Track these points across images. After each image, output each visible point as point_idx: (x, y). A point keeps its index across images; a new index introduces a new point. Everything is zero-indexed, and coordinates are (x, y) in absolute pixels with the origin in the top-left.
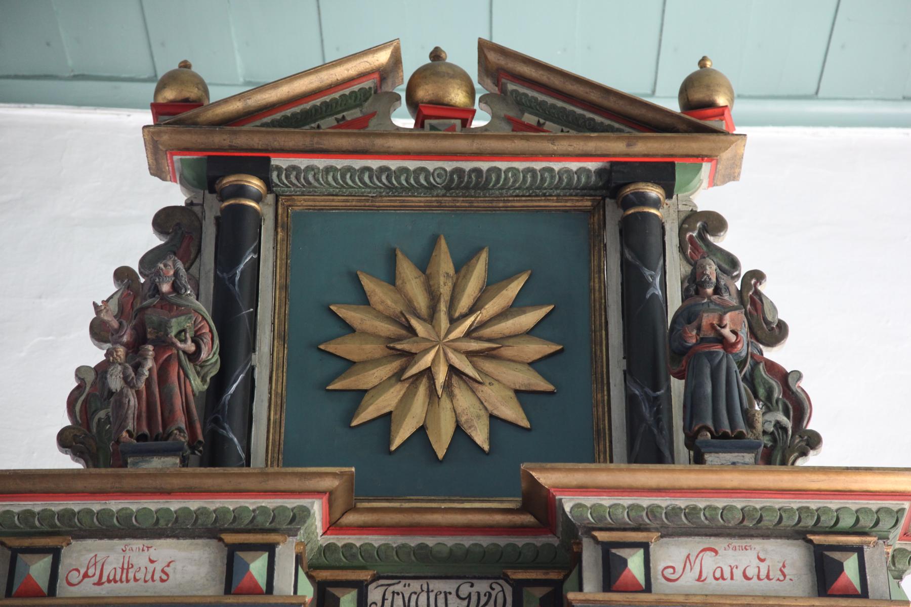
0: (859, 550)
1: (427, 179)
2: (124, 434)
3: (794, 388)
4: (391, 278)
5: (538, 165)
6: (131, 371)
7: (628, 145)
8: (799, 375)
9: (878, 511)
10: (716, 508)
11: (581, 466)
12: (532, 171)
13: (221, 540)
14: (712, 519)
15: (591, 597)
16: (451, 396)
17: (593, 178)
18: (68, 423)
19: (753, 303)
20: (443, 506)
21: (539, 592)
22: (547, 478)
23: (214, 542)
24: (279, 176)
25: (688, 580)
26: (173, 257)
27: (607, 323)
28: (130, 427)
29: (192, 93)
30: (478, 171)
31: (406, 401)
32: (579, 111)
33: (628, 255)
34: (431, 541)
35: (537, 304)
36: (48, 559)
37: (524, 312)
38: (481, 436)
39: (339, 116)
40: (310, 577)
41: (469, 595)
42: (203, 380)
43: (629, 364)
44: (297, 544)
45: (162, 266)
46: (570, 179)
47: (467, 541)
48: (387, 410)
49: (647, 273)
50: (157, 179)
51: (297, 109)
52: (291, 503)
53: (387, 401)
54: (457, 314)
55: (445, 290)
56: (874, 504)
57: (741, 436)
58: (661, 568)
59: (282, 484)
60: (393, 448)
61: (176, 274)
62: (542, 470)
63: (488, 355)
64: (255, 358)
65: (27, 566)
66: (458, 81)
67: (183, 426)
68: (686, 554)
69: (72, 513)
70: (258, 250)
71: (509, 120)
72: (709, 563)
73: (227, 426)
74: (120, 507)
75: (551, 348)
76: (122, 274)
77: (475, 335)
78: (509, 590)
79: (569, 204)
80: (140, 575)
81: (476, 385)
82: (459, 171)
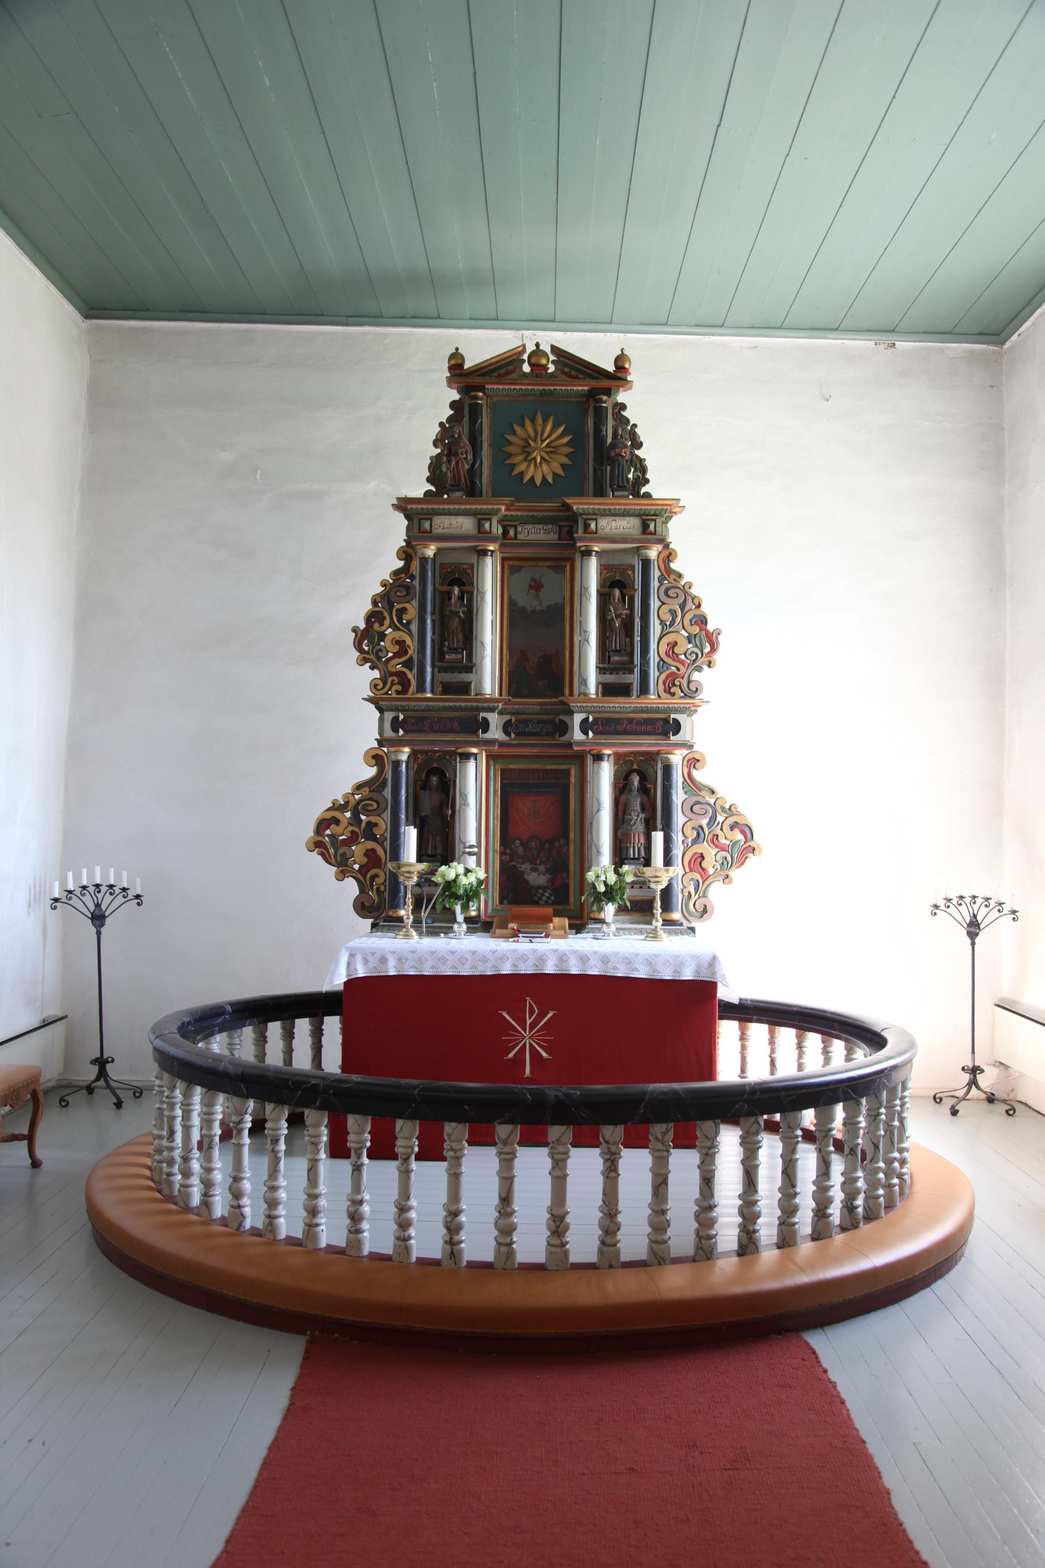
0: (655, 520)
4: (523, 426)
5: (569, 388)
8: (645, 460)
12: (567, 390)
21: (566, 529)
25: (608, 529)
29: (460, 361)
30: (550, 390)
31: (528, 467)
34: (535, 514)
35: (568, 435)
36: (429, 522)
38: (550, 479)
47: (546, 514)
49: (602, 427)
52: (496, 507)
53: (522, 467)
55: (540, 430)
56: (660, 508)
57: (625, 486)
70: (482, 418)
72: (614, 524)
76: (441, 424)
78: (557, 527)
82: (544, 390)
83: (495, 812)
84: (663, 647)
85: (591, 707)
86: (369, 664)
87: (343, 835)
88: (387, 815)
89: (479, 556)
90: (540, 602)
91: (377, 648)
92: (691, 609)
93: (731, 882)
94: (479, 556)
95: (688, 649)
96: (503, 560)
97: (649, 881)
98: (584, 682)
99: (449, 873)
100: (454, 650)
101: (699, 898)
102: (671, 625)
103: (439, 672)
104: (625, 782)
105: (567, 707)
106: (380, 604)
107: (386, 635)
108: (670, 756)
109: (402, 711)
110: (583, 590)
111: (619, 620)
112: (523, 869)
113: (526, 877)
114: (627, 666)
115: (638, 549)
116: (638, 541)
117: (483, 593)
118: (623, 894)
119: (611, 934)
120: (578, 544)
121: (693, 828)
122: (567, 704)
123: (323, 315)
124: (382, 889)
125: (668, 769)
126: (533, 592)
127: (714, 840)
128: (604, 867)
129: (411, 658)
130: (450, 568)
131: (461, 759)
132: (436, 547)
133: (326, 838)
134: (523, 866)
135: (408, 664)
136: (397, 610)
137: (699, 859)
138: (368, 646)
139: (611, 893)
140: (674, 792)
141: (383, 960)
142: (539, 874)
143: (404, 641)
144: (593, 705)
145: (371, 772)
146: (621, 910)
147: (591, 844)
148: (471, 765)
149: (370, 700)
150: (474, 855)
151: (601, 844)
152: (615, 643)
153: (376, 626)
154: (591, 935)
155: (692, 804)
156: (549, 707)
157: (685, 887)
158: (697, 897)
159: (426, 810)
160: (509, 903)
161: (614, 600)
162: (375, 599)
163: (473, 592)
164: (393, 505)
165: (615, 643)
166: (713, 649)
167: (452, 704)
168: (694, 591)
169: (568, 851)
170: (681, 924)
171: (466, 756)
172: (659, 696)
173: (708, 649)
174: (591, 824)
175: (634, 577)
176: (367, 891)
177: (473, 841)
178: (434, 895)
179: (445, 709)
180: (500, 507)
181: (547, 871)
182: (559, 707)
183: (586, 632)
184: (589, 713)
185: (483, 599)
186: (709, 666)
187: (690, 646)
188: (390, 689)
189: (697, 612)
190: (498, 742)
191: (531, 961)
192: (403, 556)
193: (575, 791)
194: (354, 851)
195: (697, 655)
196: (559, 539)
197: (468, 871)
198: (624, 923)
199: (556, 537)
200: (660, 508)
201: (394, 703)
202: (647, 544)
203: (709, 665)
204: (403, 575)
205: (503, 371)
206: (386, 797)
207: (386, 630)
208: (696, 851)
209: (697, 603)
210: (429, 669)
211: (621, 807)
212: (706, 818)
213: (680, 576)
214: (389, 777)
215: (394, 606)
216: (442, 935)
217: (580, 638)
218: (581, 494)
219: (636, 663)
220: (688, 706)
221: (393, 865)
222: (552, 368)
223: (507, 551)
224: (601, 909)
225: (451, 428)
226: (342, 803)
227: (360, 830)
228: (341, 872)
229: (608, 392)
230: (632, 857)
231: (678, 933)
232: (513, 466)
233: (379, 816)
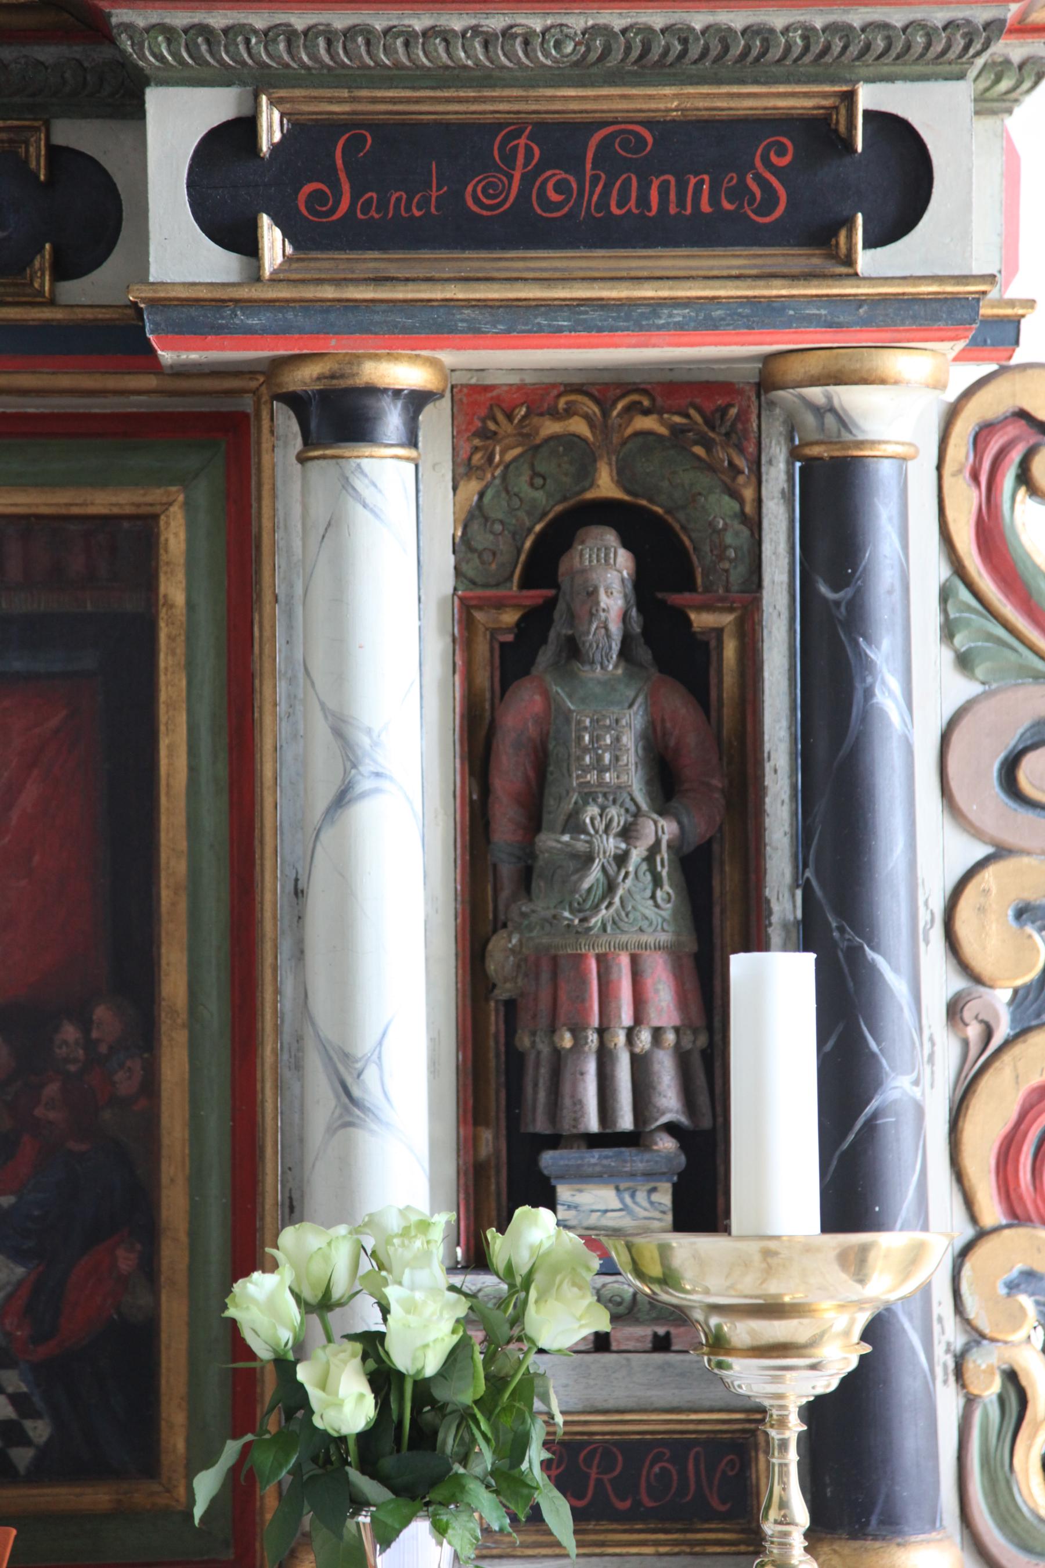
85: (268, 35)
97: (718, 1344)
104: (536, 596)
147: (299, 1039)
151: (365, 1045)
155: (1010, 741)
157: (977, 1336)
174: (299, 893)
182: (47, 53)
193: (190, 666)
230: (593, 1124)
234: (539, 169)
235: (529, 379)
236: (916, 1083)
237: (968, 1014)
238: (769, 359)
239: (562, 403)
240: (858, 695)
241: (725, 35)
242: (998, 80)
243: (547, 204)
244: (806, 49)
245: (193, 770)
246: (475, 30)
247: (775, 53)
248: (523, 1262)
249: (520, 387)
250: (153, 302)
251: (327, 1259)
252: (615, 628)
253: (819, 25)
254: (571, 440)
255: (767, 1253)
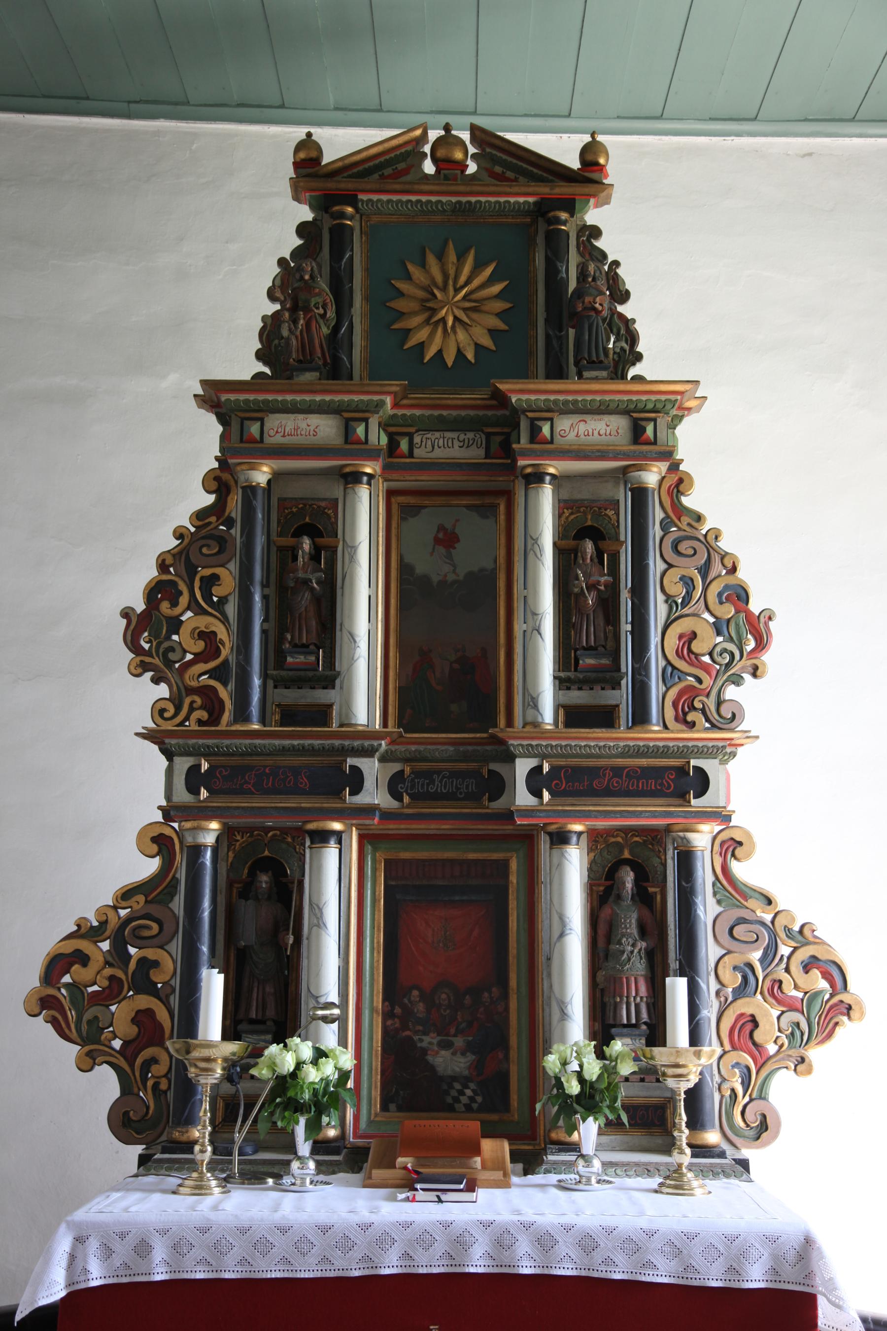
0: (655, 420)
1: (442, 206)
2: (291, 360)
3: (631, 328)
4: (423, 264)
5: (502, 199)
6: (292, 326)
7: (551, 189)
8: (634, 321)
9: (666, 400)
10: (587, 401)
11: (521, 381)
12: (499, 202)
13: (341, 415)
14: (585, 406)
15: (523, 446)
16: (455, 333)
17: (532, 207)
18: (259, 346)
19: (613, 279)
20: (451, 396)
21: (499, 439)
22: (503, 387)
23: (338, 416)
24: (362, 205)
25: (572, 436)
26: (310, 260)
27: (537, 290)
28: (294, 357)
29: (314, 154)
30: (469, 202)
31: (432, 335)
32: (525, 166)
33: (549, 254)
34: (445, 413)
35: (500, 280)
36: (258, 424)
37: (493, 285)
38: (470, 356)
39: (394, 167)
40: (385, 430)
41: (464, 440)
42: (328, 328)
43: (548, 314)
44: (379, 418)
45: (304, 265)
46: (519, 207)
47: (463, 413)
48: (422, 340)
49: (559, 264)
50: (296, 203)
51: (371, 164)
52: (376, 398)
53: (422, 335)
54: (458, 286)
55: (452, 272)
56: (663, 398)
57: (601, 362)
58: (558, 430)
59: (372, 389)
60: (425, 361)
61: (312, 269)
62: (501, 383)
63: (475, 309)
64: (353, 310)
65: (249, 428)
66: (459, 147)
67: (320, 355)
68: (570, 425)
69: (268, 401)
70: (352, 250)
71: (487, 170)
72: (582, 427)
73: (340, 351)
74: (291, 398)
75: (508, 305)
76: (282, 262)
77: (468, 298)
78: (483, 437)
79: (518, 220)
80: (303, 433)
81: (468, 327)
82: (459, 202)
83: (375, 938)
84: (672, 642)
85: (546, 746)
86: (151, 673)
87: (94, 983)
88: (176, 946)
89: (347, 483)
90: (455, 566)
91: (166, 645)
92: (719, 576)
93: (809, 1071)
94: (347, 483)
95: (716, 645)
96: (390, 494)
97: (664, 1074)
98: (533, 703)
99: (283, 1061)
100: (302, 648)
101: (751, 1100)
102: (685, 604)
103: (275, 687)
104: (609, 883)
105: (504, 747)
106: (172, 569)
107: (182, 622)
108: (690, 835)
109: (206, 755)
110: (530, 542)
111: (594, 594)
112: (424, 1044)
113: (430, 1058)
114: (608, 675)
115: (625, 470)
116: (626, 456)
117: (353, 547)
118: (615, 1100)
119: (593, 1180)
120: (521, 463)
121: (735, 968)
122: (502, 742)
123: (88, 98)
124: (164, 1086)
125: (686, 859)
126: (441, 550)
127: (775, 990)
128: (576, 1044)
129: (226, 662)
130: (297, 507)
131: (312, 842)
132: (272, 468)
133: (63, 991)
134: (424, 1037)
135: (220, 674)
136: (202, 578)
137: (749, 1027)
138: (149, 642)
139: (592, 1097)
140: (699, 900)
141: (143, 1249)
142: (454, 1054)
143: (214, 633)
144: (549, 742)
145: (151, 866)
146: (611, 1126)
147: (550, 998)
148: (331, 855)
149: (149, 736)
150: (333, 1021)
151: (568, 999)
152: (587, 635)
153: (165, 607)
154: (553, 1178)
155: (731, 923)
156: (470, 748)
157: (724, 1080)
158: (747, 1099)
159: (248, 936)
160: (400, 1109)
161: (584, 560)
162: (164, 560)
163: (337, 547)
164: (195, 396)
165: (587, 635)
166: (762, 644)
167: (296, 742)
168: (724, 544)
169: (507, 1009)
170: (722, 1155)
171: (322, 837)
172: (665, 727)
173: (751, 645)
174: (549, 959)
175: (618, 521)
176: (136, 1090)
177: (333, 996)
178: (259, 1096)
179: (284, 751)
180: (382, 397)
181: (469, 1048)
182: (488, 748)
183: (535, 614)
184: (544, 757)
185: (353, 558)
186: (754, 675)
187: (720, 639)
188: (187, 718)
189: (730, 580)
190: (380, 810)
191: (439, 1248)
192: (214, 485)
193: (518, 898)
194: (113, 1014)
195: (732, 655)
196: (487, 456)
197: (320, 1054)
198: (613, 1150)
199: (482, 452)
200: (663, 398)
201: (192, 742)
202: (642, 461)
203: (755, 672)
204: (213, 519)
205: (388, 171)
206: (176, 912)
207: (182, 614)
208: (743, 1011)
209: (730, 565)
210: (257, 682)
211: (602, 929)
212: (757, 949)
213: (699, 518)
214: (182, 875)
215: (196, 572)
216: (270, 1181)
217: (524, 627)
218: (524, 373)
219: (623, 669)
220: (720, 744)
221: (177, 1046)
222: (472, 168)
223: (395, 476)
224: (574, 1127)
225: (299, 268)
226: (95, 924)
227: (126, 974)
228: (89, 1054)
229: (570, 206)
231: (718, 1174)
232: (407, 333)
233: (162, 947)
234: (612, 778)
235: (607, 827)
236: (709, 1012)
237: (721, 994)
238: (668, 825)
239: (615, 833)
240: (693, 911)
241: (658, 747)
242: (724, 756)
243: (614, 787)
244: (678, 751)
245: (518, 926)
246: (597, 745)
247: (670, 751)
248: (614, 1054)
249: (605, 829)
250: (517, 810)
251: (565, 1052)
252: (630, 892)
253: (681, 745)
254: (617, 843)
255: (677, 1052)
